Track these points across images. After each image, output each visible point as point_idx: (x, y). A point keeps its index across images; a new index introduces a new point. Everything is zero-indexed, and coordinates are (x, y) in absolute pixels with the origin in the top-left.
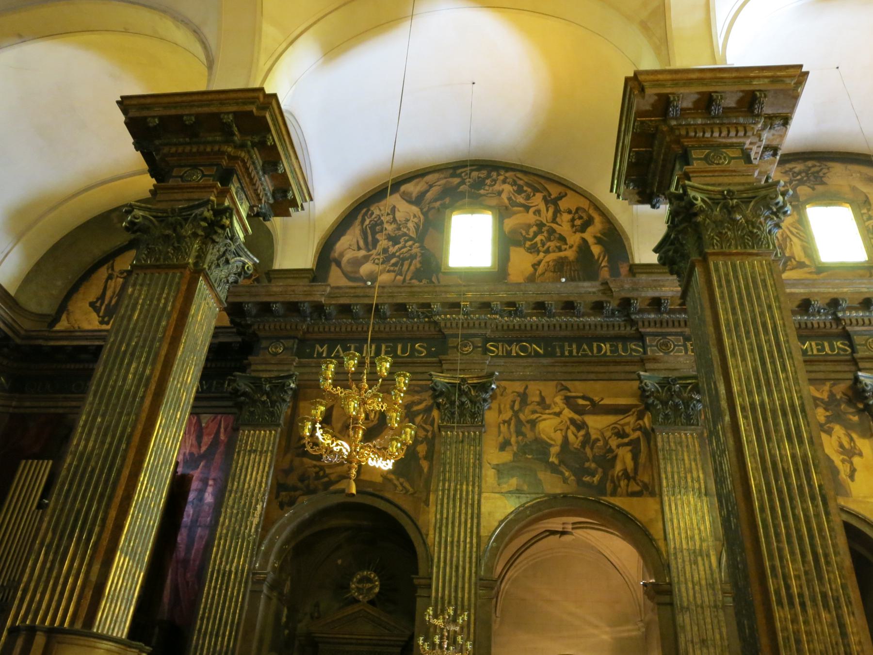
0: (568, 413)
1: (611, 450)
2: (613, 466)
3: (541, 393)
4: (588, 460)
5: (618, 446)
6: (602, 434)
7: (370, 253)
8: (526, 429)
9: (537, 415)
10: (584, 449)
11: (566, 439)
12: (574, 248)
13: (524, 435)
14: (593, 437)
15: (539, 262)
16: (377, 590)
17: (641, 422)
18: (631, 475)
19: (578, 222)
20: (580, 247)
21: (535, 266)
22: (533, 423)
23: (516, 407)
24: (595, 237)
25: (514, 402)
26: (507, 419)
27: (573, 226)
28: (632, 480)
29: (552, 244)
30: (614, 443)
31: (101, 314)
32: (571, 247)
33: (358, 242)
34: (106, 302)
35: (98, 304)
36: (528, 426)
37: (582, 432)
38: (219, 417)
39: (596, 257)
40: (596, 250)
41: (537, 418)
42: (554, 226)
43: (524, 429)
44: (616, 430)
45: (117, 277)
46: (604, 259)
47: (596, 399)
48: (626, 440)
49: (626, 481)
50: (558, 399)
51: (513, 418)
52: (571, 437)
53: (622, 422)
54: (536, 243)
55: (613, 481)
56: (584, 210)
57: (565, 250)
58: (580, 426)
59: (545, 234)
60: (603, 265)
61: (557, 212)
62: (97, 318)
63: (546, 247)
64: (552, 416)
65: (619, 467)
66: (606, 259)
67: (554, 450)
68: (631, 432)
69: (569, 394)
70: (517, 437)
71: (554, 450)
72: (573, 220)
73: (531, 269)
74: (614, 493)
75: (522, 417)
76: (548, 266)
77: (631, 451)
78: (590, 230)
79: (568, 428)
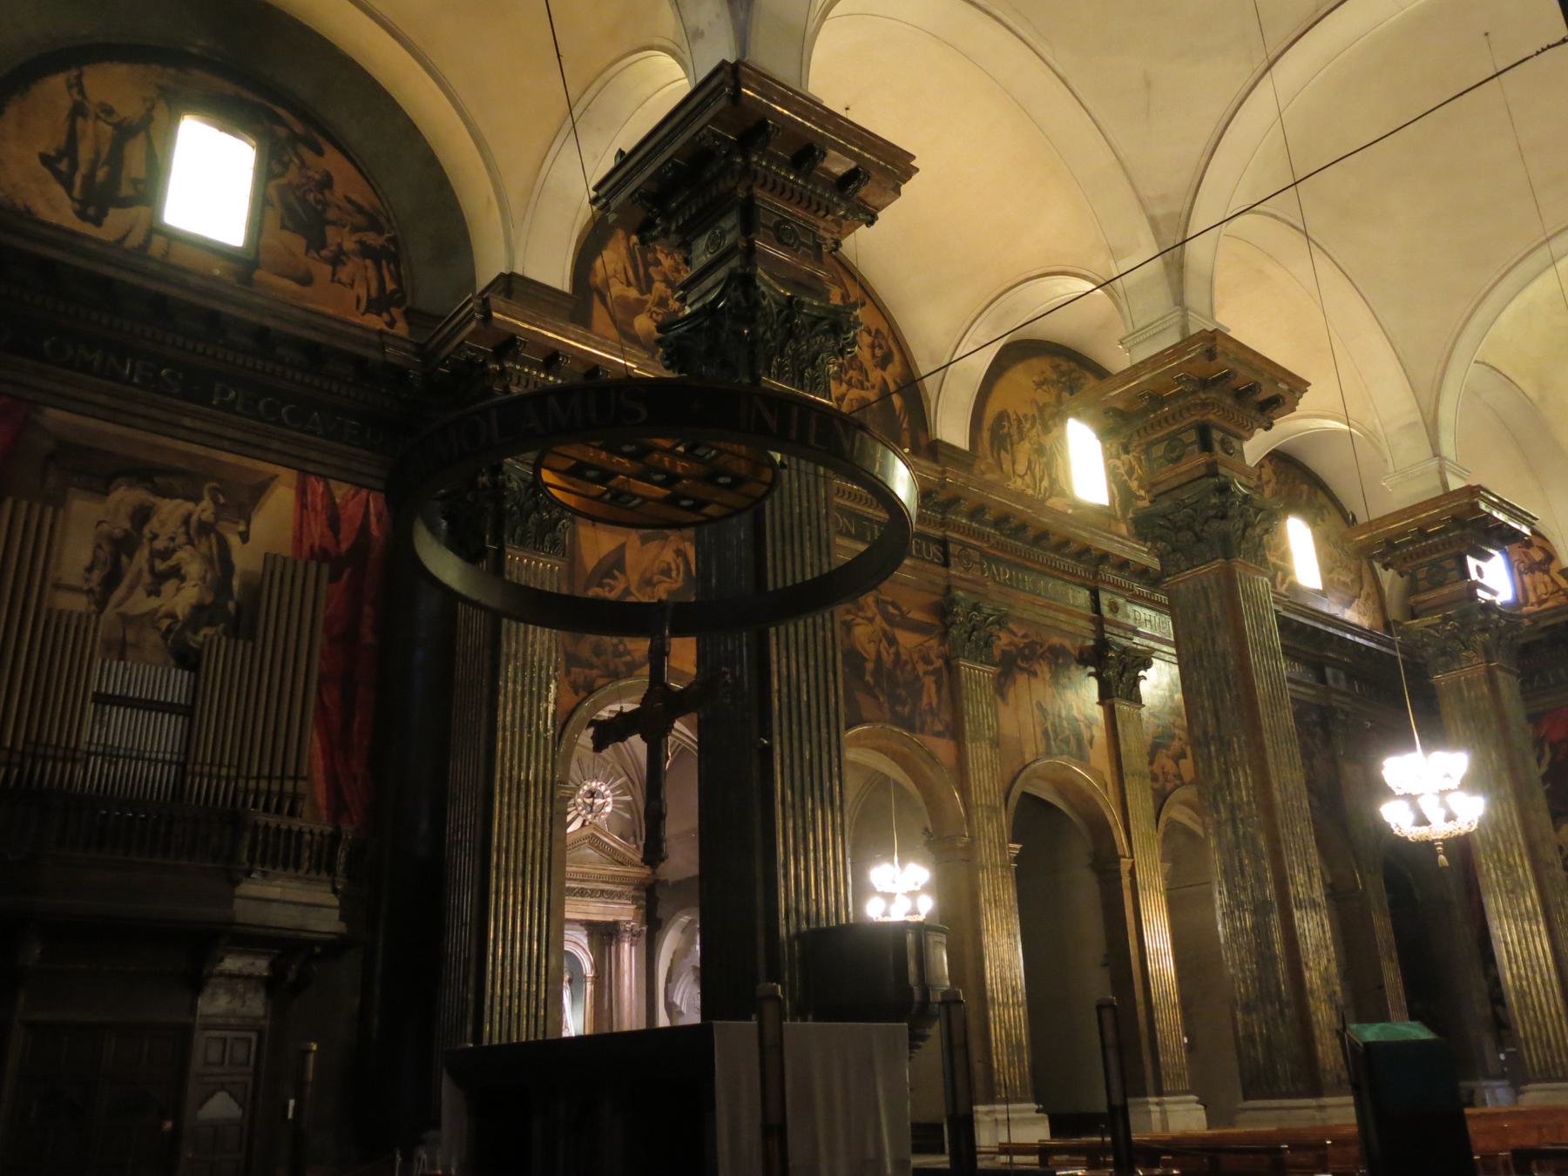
1: (917, 678)
5: (926, 673)
6: (911, 655)
7: (645, 297)
9: (852, 617)
11: (879, 653)
12: (876, 391)
14: (904, 657)
16: (608, 809)
17: (942, 648)
19: (878, 352)
24: (895, 382)
27: (874, 356)
30: (921, 668)
31: (77, 192)
32: (873, 387)
33: (625, 268)
34: (83, 169)
35: (63, 166)
37: (892, 650)
38: (364, 493)
39: (897, 413)
40: (897, 400)
45: (97, 117)
47: (904, 609)
48: (930, 668)
57: (868, 389)
58: (892, 641)
62: (68, 201)
63: (848, 376)
64: (865, 622)
65: (925, 700)
67: (870, 666)
69: (881, 597)
71: (870, 666)
72: (872, 347)
74: (922, 731)
77: (936, 682)
78: (890, 368)
79: (880, 641)
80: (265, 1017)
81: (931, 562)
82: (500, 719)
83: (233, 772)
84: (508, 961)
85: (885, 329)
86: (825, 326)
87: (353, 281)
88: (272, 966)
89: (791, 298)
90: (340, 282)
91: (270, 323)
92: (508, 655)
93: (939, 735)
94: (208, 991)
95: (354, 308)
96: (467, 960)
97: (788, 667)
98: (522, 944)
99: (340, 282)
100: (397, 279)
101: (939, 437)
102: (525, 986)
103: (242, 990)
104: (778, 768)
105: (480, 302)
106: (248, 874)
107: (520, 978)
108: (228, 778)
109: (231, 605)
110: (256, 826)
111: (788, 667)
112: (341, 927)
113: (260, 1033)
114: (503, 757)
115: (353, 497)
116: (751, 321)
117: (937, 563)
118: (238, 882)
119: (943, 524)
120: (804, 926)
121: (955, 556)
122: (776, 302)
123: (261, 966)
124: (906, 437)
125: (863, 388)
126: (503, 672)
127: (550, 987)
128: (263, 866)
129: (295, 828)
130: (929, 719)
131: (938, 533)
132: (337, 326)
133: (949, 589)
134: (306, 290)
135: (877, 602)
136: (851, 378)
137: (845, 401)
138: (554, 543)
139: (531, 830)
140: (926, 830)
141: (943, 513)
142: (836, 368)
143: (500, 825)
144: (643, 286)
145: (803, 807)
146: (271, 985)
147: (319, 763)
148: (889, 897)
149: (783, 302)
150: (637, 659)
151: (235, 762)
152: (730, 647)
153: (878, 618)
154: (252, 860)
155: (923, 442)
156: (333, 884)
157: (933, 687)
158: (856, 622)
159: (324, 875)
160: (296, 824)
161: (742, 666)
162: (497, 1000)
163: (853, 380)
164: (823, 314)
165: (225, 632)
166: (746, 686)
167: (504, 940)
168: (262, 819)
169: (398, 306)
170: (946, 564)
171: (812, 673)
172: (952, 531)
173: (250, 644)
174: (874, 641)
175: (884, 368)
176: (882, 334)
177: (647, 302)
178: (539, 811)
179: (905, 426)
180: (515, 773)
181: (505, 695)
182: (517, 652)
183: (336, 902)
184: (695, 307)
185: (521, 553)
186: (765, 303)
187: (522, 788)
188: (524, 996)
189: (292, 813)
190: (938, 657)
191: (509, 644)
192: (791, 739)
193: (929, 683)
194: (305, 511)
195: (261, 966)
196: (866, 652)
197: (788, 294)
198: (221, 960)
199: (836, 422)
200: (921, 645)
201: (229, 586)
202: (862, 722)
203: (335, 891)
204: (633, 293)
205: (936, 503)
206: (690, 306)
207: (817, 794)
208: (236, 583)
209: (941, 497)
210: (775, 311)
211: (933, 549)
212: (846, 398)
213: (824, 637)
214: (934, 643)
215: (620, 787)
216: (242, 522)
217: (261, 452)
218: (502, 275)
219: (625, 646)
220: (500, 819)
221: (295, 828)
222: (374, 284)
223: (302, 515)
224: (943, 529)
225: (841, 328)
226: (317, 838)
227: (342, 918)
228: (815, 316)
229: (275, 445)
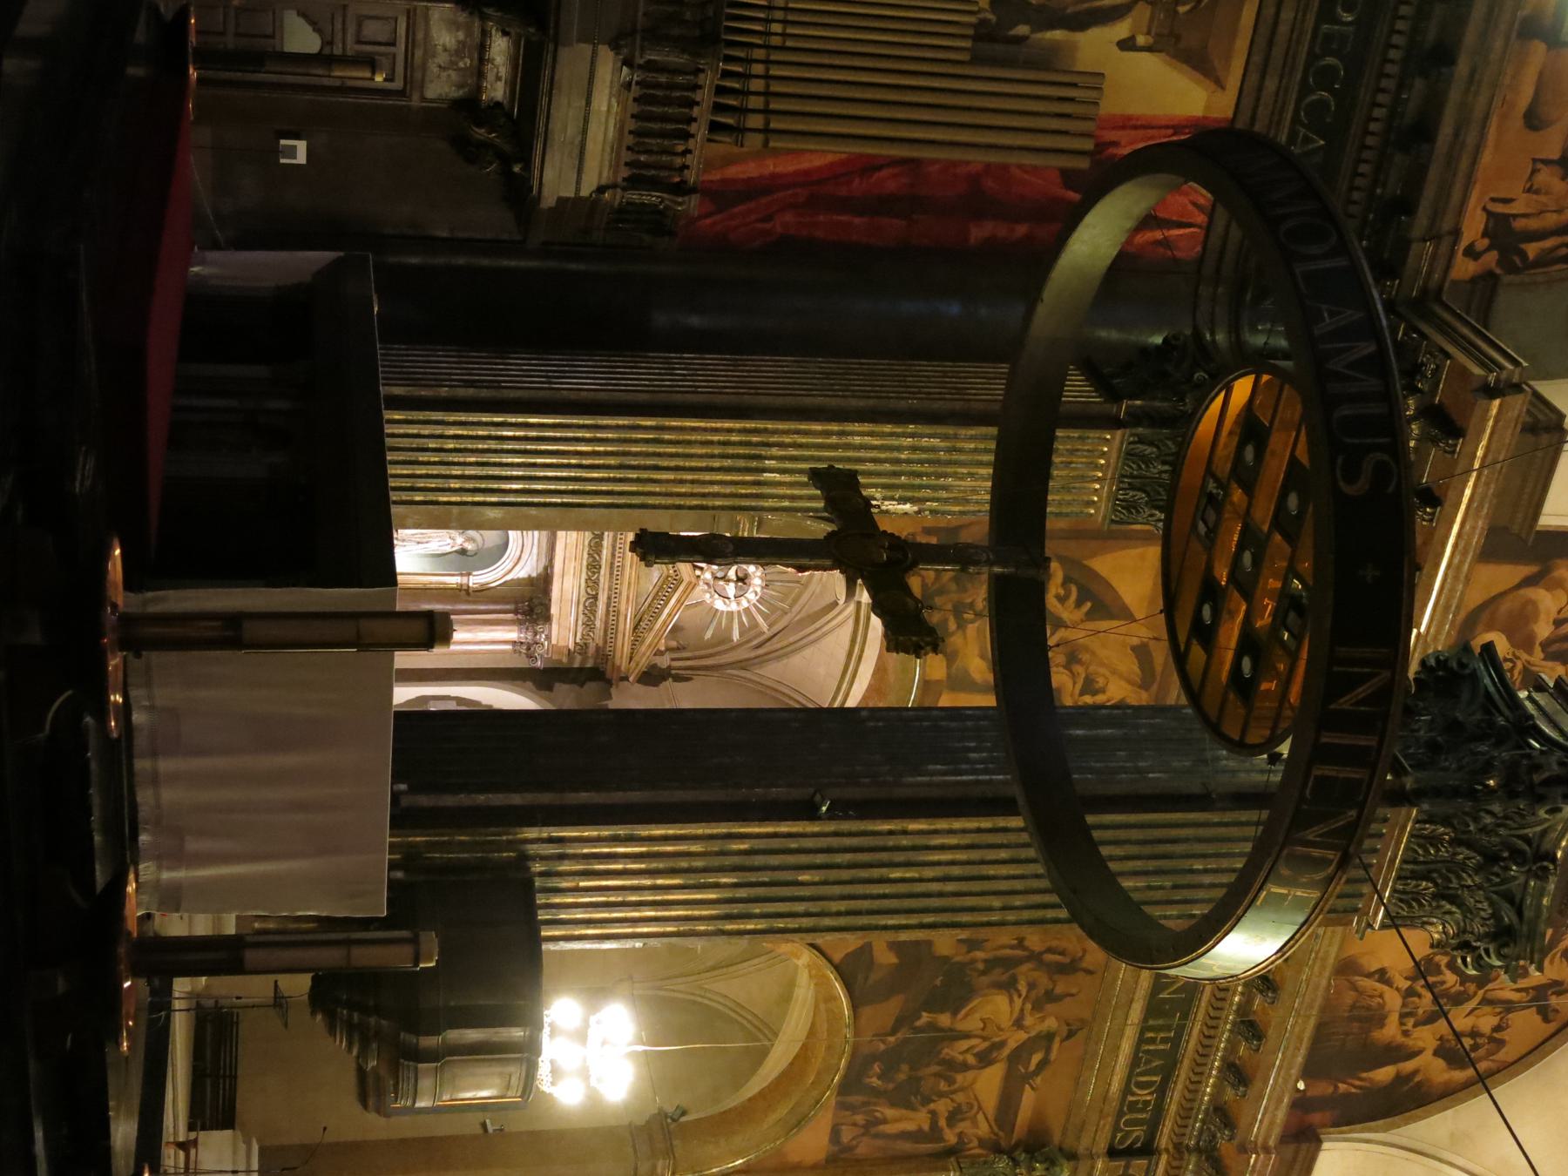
0: (1016, 1039)
1: (926, 1101)
2: (893, 1105)
3: (1072, 995)
4: (912, 1069)
5: (933, 1113)
6: (962, 1089)
7: (1538, 649)
8: (997, 975)
10: (939, 1064)
11: (967, 1036)
12: (1400, 1039)
13: (984, 973)
14: (959, 1078)
15: (1388, 983)
16: (719, 604)
17: (975, 1143)
18: (873, 1130)
20: (1400, 1047)
21: (1382, 976)
22: (1009, 986)
23: (1049, 957)
24: (1416, 1072)
25: (1062, 953)
26: (1027, 943)
28: (862, 1130)
29: (1426, 1002)
30: (942, 1107)
32: (1406, 1033)
36: (1005, 978)
37: (971, 1059)
38: (1201, 219)
39: (1364, 1075)
40: (1385, 1074)
41: (1018, 991)
42: (1473, 1004)
43: (998, 971)
44: (964, 1108)
46: (1355, 1087)
47: (1038, 1080)
48: (942, 1123)
49: (862, 1122)
50: (1051, 1023)
51: (1026, 953)
52: (964, 1044)
53: (980, 1117)
54: (1440, 972)
55: (865, 1104)
56: (1490, 1053)
57: (1402, 1024)
58: (985, 1059)
59: (1458, 988)
60: (1340, 1085)
61: (1509, 1007)
64: (1015, 1015)
65: (890, 1113)
66: (1353, 1090)
67: (944, 1020)
68: (957, 1130)
69: (1057, 1040)
70: (986, 961)
72: (1474, 1034)
73: (1374, 967)
74: (842, 1106)
75: (1025, 967)
76: (1372, 997)
77: (920, 1130)
78: (1440, 1063)
79: (984, 1039)
80: (423, 99)
81: (1116, 1128)
82: (857, 427)
83: (776, 41)
84: (493, 445)
85: (1505, 1055)
86: (1508, 916)
87: (1537, 192)
88: (498, 104)
89: (1553, 859)
90: (1534, 171)
91: (1462, 67)
92: (956, 437)
93: (835, 1133)
94: (462, 17)
95: (1493, 195)
96: (496, 385)
97: (942, 848)
98: (519, 465)
99: (1534, 171)
100: (1544, 260)
101: (1326, 1145)
102: (457, 471)
103: (461, 65)
104: (784, 828)
105: (1516, 379)
106: (627, 62)
107: (470, 464)
108: (769, 34)
109: (1022, 30)
110: (698, 71)
111: (942, 848)
112: (548, 200)
113: (401, 93)
114: (798, 432)
115: (1194, 204)
116: (1509, 791)
117: (1114, 1137)
118: (615, 46)
119: (1179, 1149)
120: (538, 867)
121: (1127, 1167)
122: (1544, 833)
123: (496, 90)
124: (1323, 1089)
125: (1403, 1016)
126: (927, 430)
127: (455, 510)
128: (638, 83)
129: (693, 128)
130: (860, 1119)
131: (1164, 1140)
132: (1464, 164)
133: (1072, 1156)
134: (1517, 122)
135: (1049, 1037)
136: (1419, 996)
137: (1378, 985)
138: (1130, 506)
139: (689, 477)
140: (684, 1113)
141: (1198, 1150)
142: (1436, 936)
143: (694, 429)
144: (1555, 647)
145: (722, 870)
146: (469, 106)
147: (788, 166)
148: (581, 1036)
149: (1546, 846)
150: (952, 639)
151: (789, 43)
152: (973, 755)
153: (1022, 1036)
154: (650, 66)
155: (1316, 1118)
156: (614, 186)
157: (910, 1126)
158: (1015, 998)
159: (625, 172)
160: (700, 130)
161: (945, 773)
162: (438, 430)
163: (1416, 999)
164: (1528, 914)
165: (983, 22)
166: (910, 779)
167: (526, 439)
168: (708, 80)
169: (1499, 263)
170: (1113, 1153)
171: (935, 887)
172: (1168, 1163)
173: (965, 57)
174: (983, 1029)
175: (1436, 1053)
176: (1498, 1051)
177: (1530, 652)
178: (716, 489)
179: (1342, 1087)
180: (775, 451)
181: (892, 434)
182: (960, 451)
183: (585, 193)
184: (1528, 704)
185: (1114, 455)
186: (1542, 813)
187: (753, 462)
188: (443, 470)
189: (715, 127)
190: (960, 1135)
191: (972, 438)
192: (829, 850)
193: (917, 1120)
194: (1170, 131)
195: (496, 90)
196: (967, 1015)
197: (1559, 854)
198: (505, 33)
199: (1353, 813)
200: (980, 1108)
201: (1052, 26)
202: (855, 1007)
203: (601, 189)
204: (1543, 630)
205: (1214, 1136)
206: (1530, 698)
207: (742, 893)
208: (1057, 35)
209: (1225, 1146)
210: (1529, 832)
211: (1138, 1132)
212: (1385, 988)
213: (990, 909)
214: (983, 1129)
215: (755, 625)
216: (1150, 40)
217: (1259, 66)
218: (1562, 416)
219: (972, 622)
220: (705, 430)
221: (693, 128)
222: (1533, 224)
223: (1167, 127)
224: (1171, 1147)
225: (1506, 945)
226: (678, 161)
227: (562, 201)
228: (1522, 900)
229: (1271, 85)
